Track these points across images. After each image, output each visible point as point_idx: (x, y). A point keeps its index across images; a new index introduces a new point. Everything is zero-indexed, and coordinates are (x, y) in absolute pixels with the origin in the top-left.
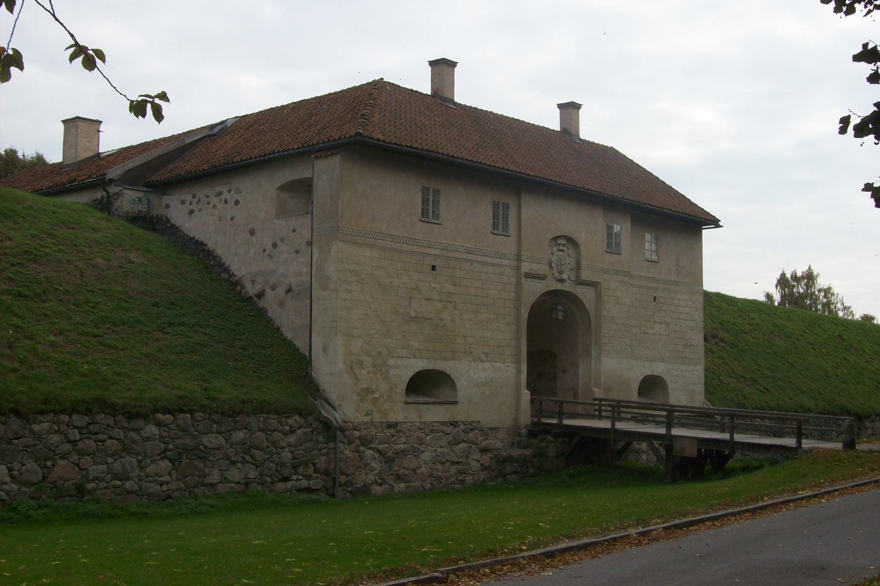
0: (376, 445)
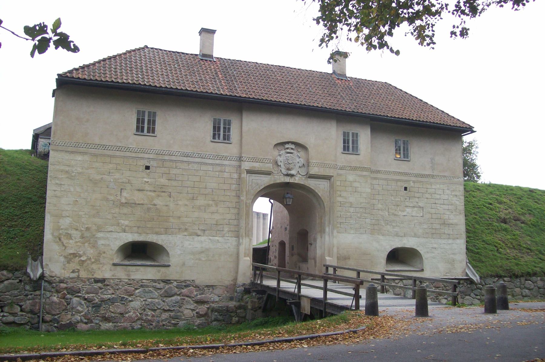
0: (83, 294)
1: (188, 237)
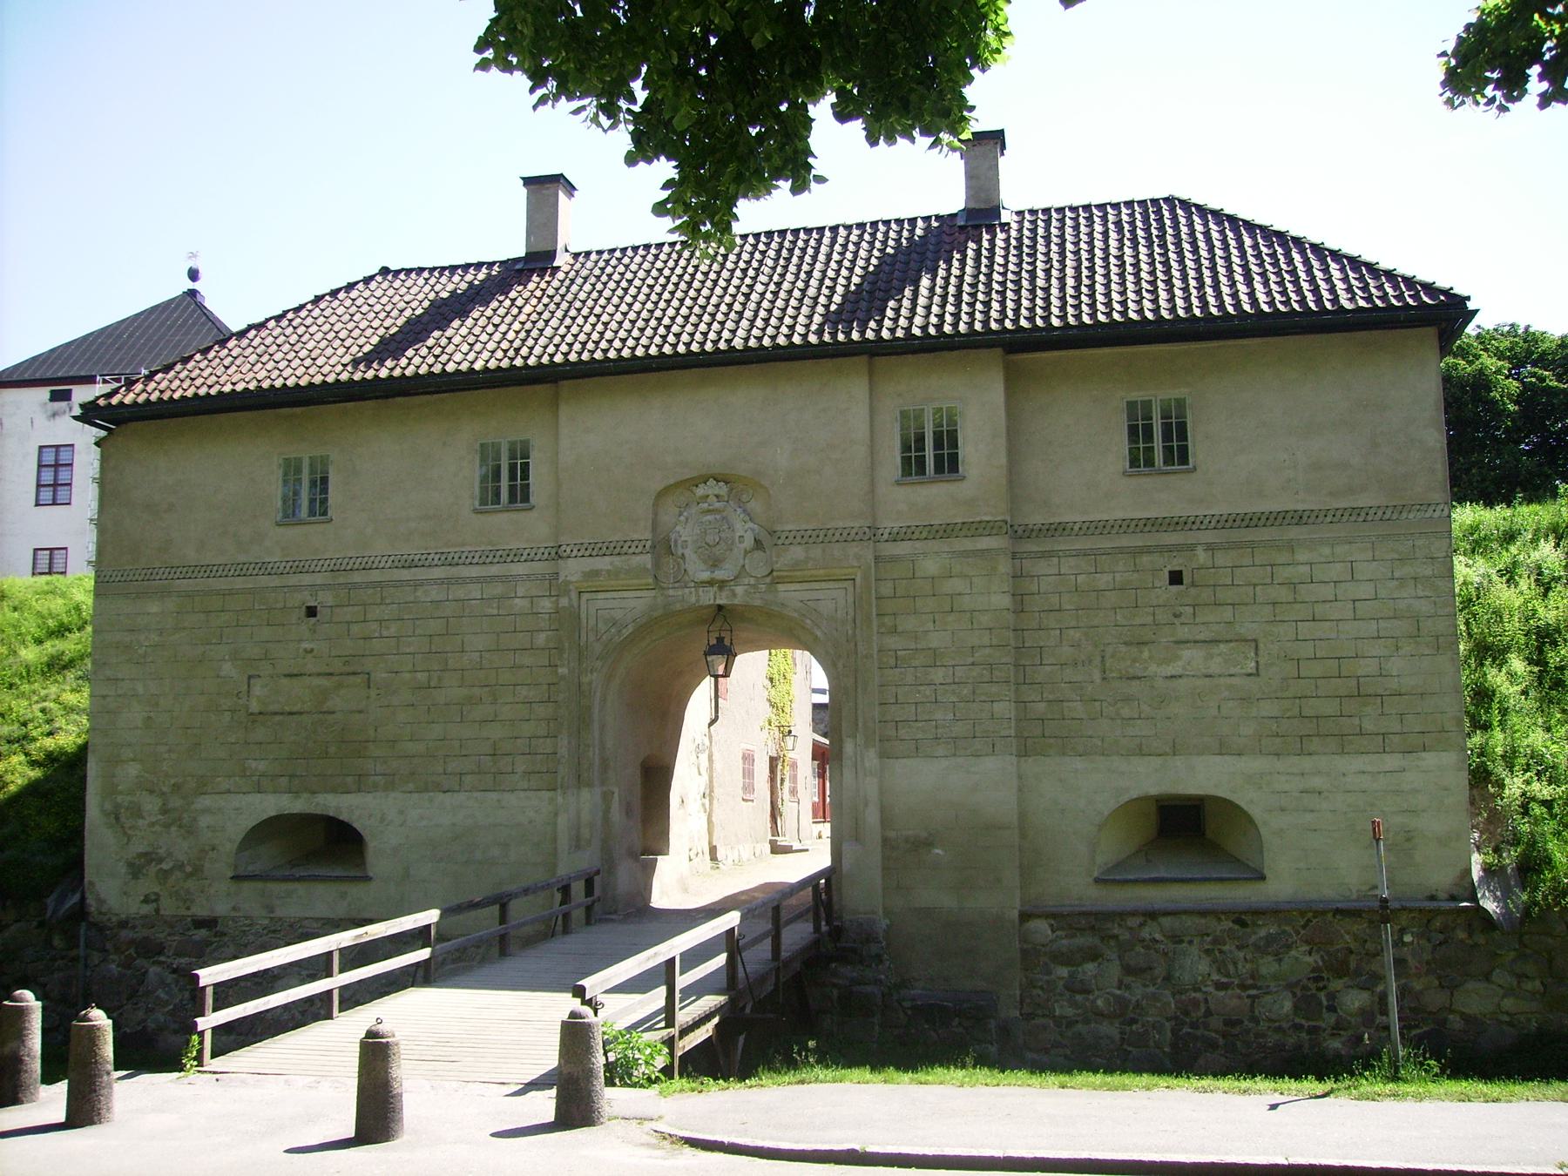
0: (169, 957)
1: (416, 795)
